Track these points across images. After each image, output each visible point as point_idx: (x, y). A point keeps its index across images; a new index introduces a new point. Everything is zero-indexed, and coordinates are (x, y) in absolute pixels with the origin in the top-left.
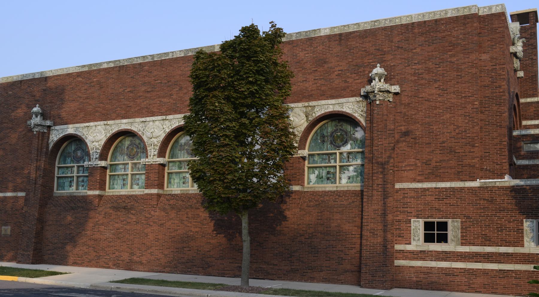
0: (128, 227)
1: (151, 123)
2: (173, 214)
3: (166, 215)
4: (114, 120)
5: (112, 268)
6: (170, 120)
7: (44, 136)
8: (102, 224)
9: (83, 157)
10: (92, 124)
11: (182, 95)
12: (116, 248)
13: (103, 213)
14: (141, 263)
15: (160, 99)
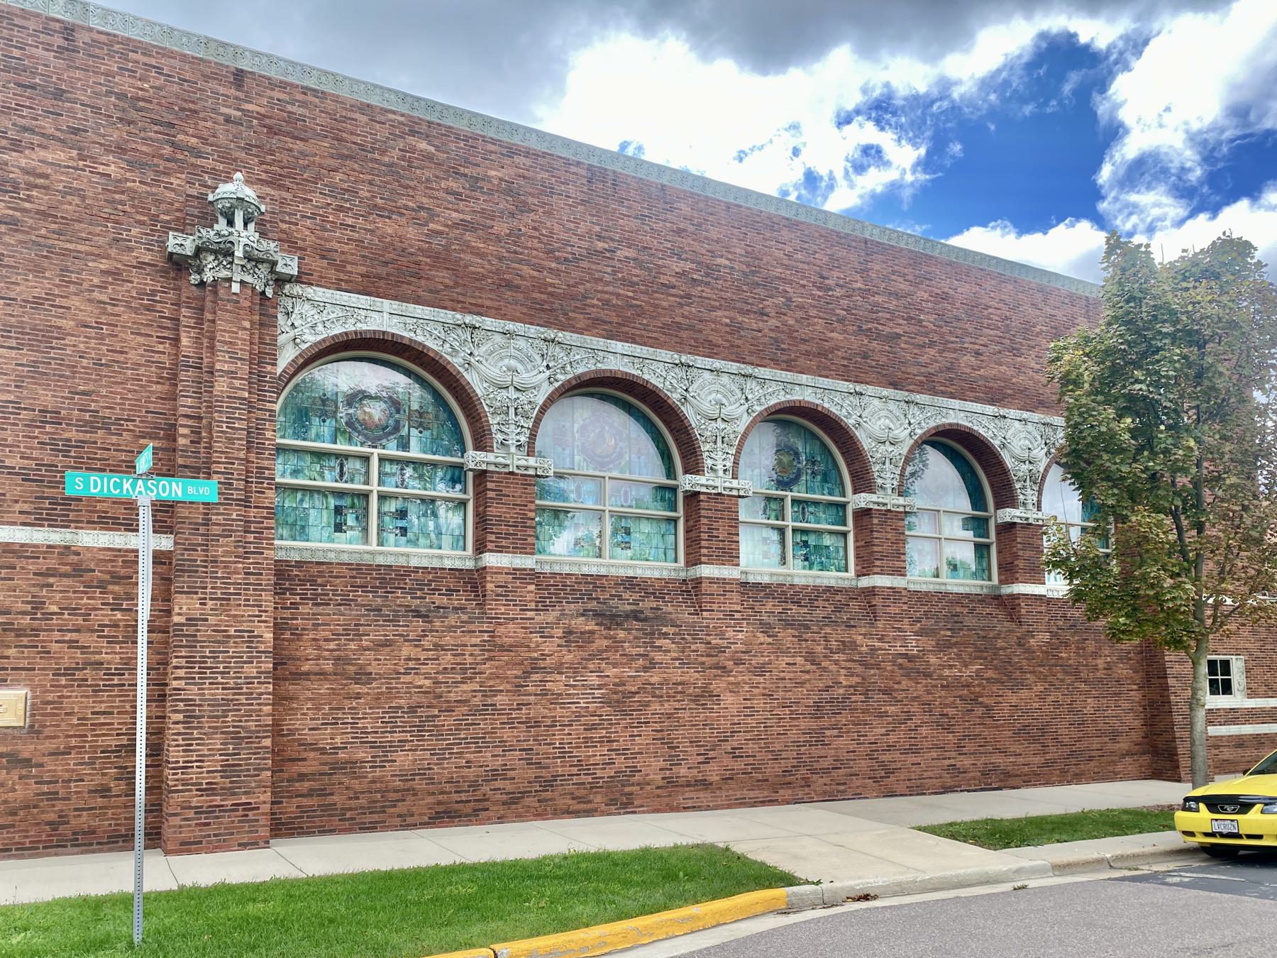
0: (655, 679)
1: (707, 375)
2: (787, 637)
3: (770, 640)
5: (603, 814)
6: (763, 382)
8: (559, 669)
11: (791, 322)
12: (615, 745)
15: (732, 314)
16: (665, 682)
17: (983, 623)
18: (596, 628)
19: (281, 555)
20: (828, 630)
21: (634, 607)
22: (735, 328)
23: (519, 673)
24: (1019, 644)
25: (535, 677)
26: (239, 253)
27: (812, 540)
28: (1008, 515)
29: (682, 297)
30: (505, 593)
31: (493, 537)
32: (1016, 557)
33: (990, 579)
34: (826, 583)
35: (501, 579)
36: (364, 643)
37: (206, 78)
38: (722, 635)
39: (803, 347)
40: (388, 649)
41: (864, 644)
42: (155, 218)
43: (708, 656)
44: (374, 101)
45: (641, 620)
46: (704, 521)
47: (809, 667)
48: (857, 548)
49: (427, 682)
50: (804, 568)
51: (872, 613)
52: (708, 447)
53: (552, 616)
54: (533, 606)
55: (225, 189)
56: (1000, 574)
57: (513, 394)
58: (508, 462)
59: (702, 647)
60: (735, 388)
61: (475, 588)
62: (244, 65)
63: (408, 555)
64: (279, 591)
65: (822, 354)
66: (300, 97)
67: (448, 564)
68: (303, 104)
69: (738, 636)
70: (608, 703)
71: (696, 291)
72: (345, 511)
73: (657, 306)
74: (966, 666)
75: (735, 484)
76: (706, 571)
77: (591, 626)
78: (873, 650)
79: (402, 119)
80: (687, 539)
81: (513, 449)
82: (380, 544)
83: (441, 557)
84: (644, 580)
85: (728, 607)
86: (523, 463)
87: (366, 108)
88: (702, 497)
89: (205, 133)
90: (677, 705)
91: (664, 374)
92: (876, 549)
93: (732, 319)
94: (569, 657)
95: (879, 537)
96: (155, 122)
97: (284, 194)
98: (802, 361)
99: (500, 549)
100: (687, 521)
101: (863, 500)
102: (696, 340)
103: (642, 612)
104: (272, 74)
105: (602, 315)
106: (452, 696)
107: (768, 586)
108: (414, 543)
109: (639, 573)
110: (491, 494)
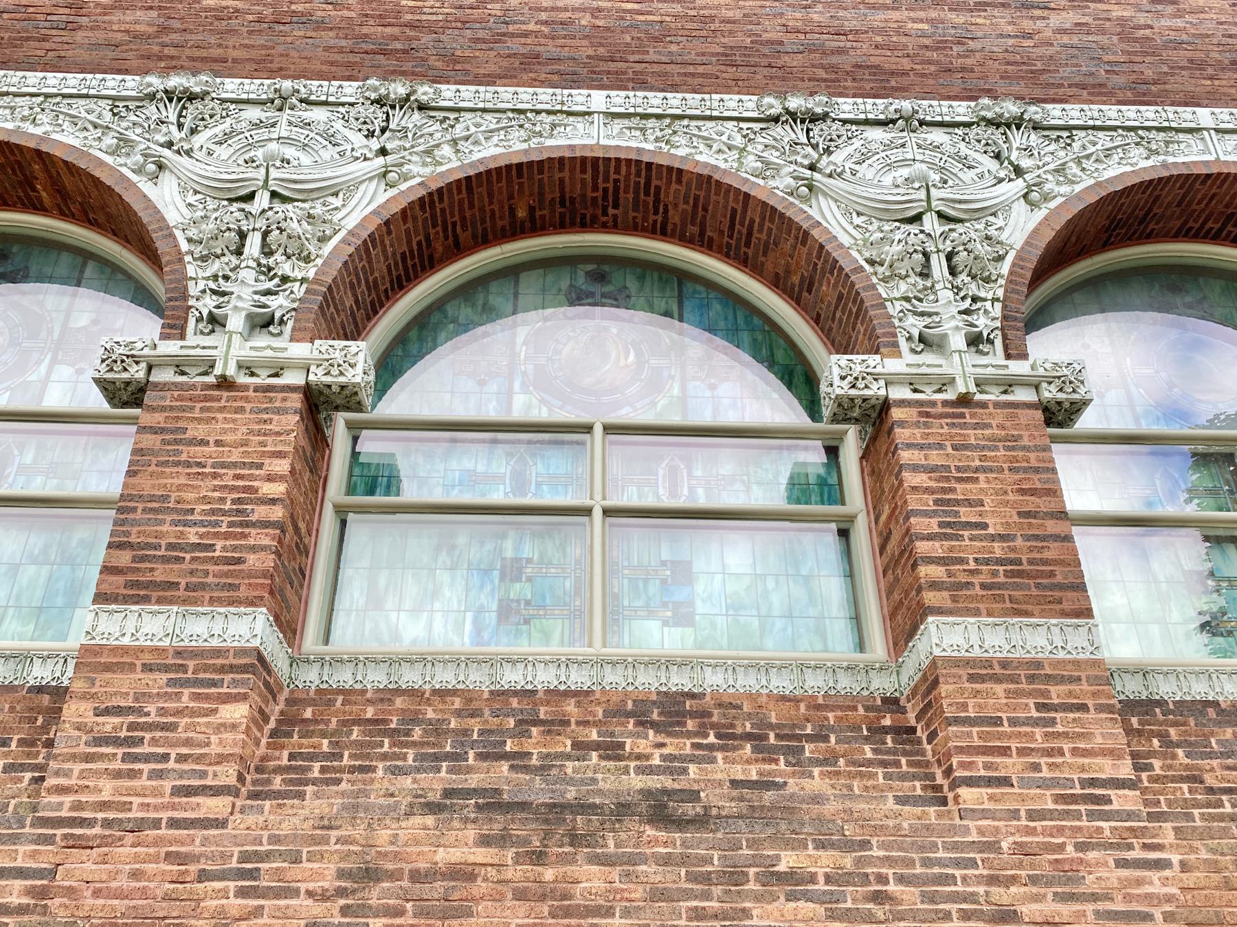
18: (481, 855)
45: (681, 824)
54: (227, 775)
85: (1072, 769)
91: (738, 141)
103: (694, 796)
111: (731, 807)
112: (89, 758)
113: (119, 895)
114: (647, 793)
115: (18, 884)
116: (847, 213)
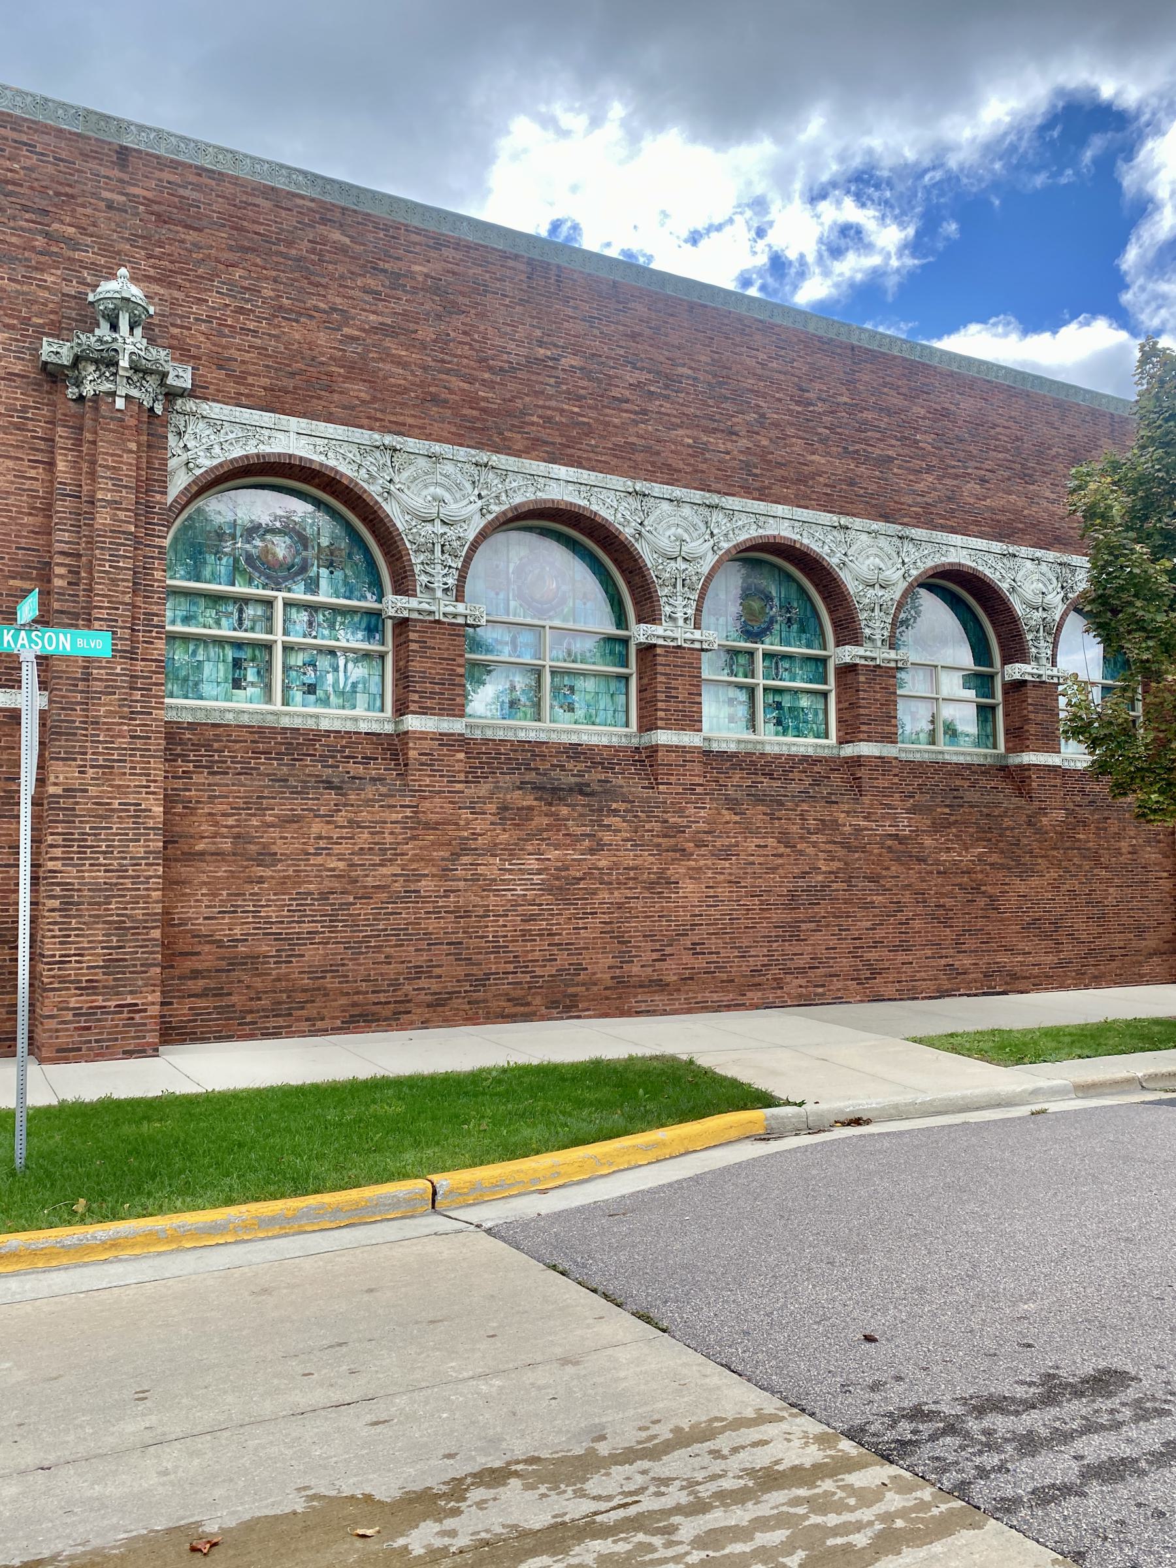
0: (603, 863)
1: (665, 505)
2: (757, 815)
3: (737, 818)
4: (518, 454)
6: (731, 514)
7: (152, 428)
8: (492, 850)
9: (304, 568)
10: (411, 444)
13: (492, 808)
14: (660, 985)
16: (615, 866)
17: (988, 798)
19: (171, 716)
20: (805, 807)
21: (578, 779)
22: (699, 450)
23: (447, 855)
24: (1030, 824)
25: (465, 859)
26: (124, 363)
27: (787, 701)
28: (1017, 671)
29: (636, 413)
30: (430, 762)
31: (416, 697)
32: (1026, 720)
33: (995, 747)
34: (802, 751)
35: (426, 745)
36: (269, 819)
37: (85, 156)
38: (681, 812)
39: (779, 472)
40: (296, 826)
41: (848, 823)
42: (26, 321)
43: (665, 836)
44: (280, 183)
45: (587, 795)
46: (660, 678)
47: (782, 850)
48: (839, 710)
49: (341, 865)
50: (777, 734)
51: (856, 786)
52: (666, 591)
53: (484, 789)
55: (109, 287)
56: (1006, 741)
57: (439, 528)
58: (433, 608)
59: (657, 827)
60: (697, 520)
61: (395, 756)
62: (128, 141)
63: (317, 717)
64: (170, 758)
65: (802, 480)
66: (192, 178)
67: (363, 727)
68: (197, 187)
69: (699, 815)
70: (550, 890)
71: (653, 406)
72: (245, 664)
73: (607, 424)
74: (967, 849)
75: (697, 635)
76: (663, 737)
77: (529, 801)
78: (858, 830)
79: (312, 205)
80: (640, 700)
81: (439, 594)
82: (286, 703)
83: (355, 720)
84: (591, 748)
86: (450, 609)
87: (270, 192)
88: (659, 651)
89: (84, 222)
90: (629, 894)
91: (615, 504)
92: (862, 711)
93: (695, 439)
94: (505, 837)
95: (866, 697)
96: (25, 208)
97: (176, 294)
98: (776, 490)
99: (424, 711)
100: (640, 678)
101: (848, 654)
102: (653, 464)
103: (588, 785)
104: (162, 152)
105: (543, 434)
106: (370, 881)
107: (735, 755)
108: (325, 702)
109: (585, 739)
110: (414, 646)
111: (600, 789)
112: (420, 770)
113: (438, 813)
114: (577, 784)
115: (409, 810)
116: (651, 551)
